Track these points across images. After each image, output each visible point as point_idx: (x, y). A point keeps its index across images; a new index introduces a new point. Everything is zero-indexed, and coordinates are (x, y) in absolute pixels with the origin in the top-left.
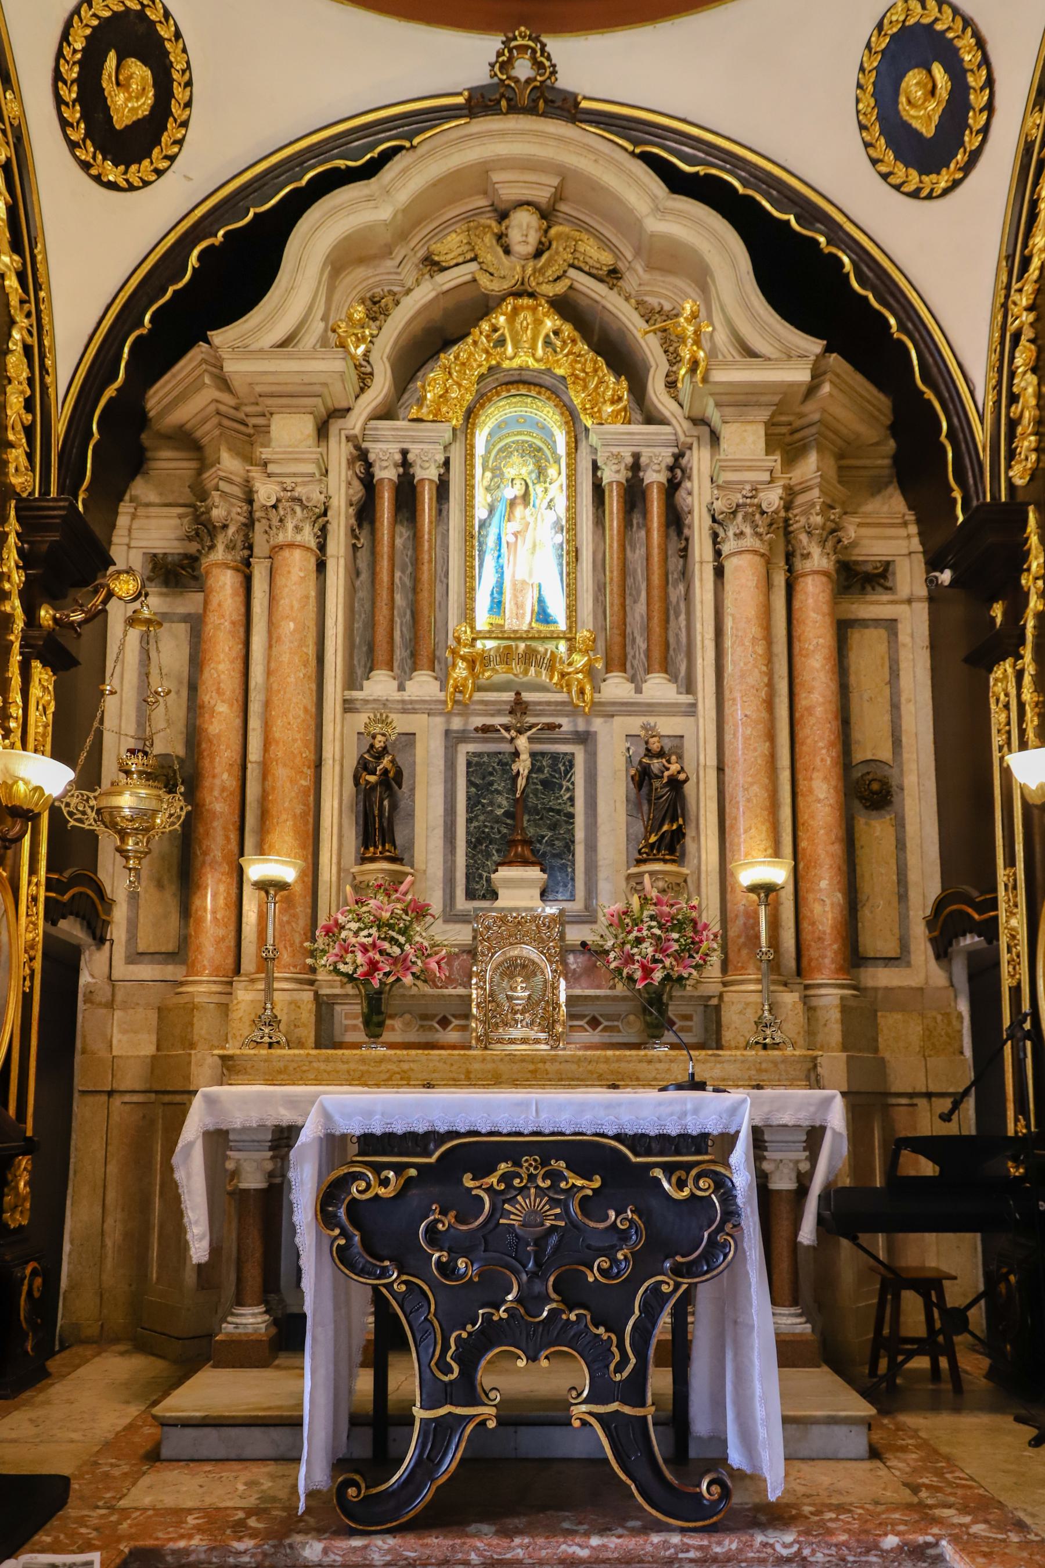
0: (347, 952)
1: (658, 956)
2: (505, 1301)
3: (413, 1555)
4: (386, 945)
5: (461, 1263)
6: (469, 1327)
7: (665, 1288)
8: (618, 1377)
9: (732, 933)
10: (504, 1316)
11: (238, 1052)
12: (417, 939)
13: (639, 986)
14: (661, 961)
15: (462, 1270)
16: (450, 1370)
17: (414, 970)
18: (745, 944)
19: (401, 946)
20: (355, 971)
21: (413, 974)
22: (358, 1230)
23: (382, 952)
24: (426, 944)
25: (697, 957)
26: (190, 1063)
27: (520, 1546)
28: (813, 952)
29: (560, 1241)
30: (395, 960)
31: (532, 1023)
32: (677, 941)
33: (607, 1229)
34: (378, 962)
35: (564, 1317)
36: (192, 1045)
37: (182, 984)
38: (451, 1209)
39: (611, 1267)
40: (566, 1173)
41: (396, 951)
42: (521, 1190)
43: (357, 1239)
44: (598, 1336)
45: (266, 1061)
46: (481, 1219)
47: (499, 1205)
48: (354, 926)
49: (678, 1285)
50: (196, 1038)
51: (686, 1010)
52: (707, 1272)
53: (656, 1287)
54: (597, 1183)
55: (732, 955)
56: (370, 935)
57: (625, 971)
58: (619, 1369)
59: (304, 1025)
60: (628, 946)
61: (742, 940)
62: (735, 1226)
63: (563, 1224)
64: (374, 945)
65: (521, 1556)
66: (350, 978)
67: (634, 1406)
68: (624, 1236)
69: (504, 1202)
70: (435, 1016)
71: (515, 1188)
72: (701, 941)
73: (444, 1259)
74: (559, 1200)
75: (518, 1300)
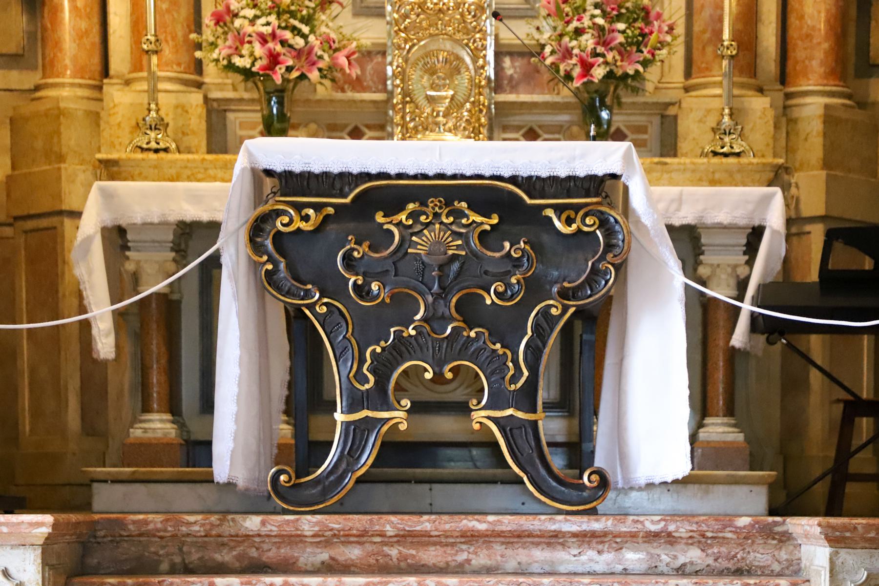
0: (242, 43)
1: (600, 49)
2: (414, 321)
3: (336, 526)
4: (288, 35)
5: (375, 286)
6: (382, 343)
7: (554, 311)
8: (513, 387)
9: (697, 28)
10: (413, 333)
11: (123, 156)
12: (323, 29)
13: (577, 84)
14: (603, 56)
15: (376, 292)
16: (368, 381)
17: (321, 65)
18: (710, 40)
19: (305, 37)
20: (253, 64)
21: (320, 70)
22: (284, 258)
23: (283, 43)
24: (333, 35)
25: (645, 50)
26: (59, 179)
27: (428, 521)
28: (798, 53)
29: (461, 268)
30: (298, 54)
31: (456, 128)
32: (623, 32)
33: (502, 257)
34: (278, 54)
35: (465, 334)
36: (61, 158)
37: (37, 88)
38: (365, 240)
39: (506, 291)
40: (467, 212)
41: (299, 42)
42: (427, 225)
43: (282, 266)
44: (494, 351)
45: (155, 167)
46: (392, 248)
47: (408, 238)
48: (250, 13)
49: (565, 309)
50: (64, 150)
51: (639, 120)
52: (590, 296)
53: (547, 309)
54: (495, 220)
55: (696, 54)
56: (268, 24)
57: (562, 67)
58: (514, 379)
59: (194, 133)
60: (566, 39)
61: (707, 35)
62: (615, 256)
63: (464, 253)
64: (273, 35)
65: (429, 528)
66: (247, 73)
67: (527, 412)
68: (517, 263)
69: (412, 234)
70: (346, 126)
71: (422, 224)
72: (651, 33)
73: (360, 282)
74: (462, 233)
75: (424, 319)
